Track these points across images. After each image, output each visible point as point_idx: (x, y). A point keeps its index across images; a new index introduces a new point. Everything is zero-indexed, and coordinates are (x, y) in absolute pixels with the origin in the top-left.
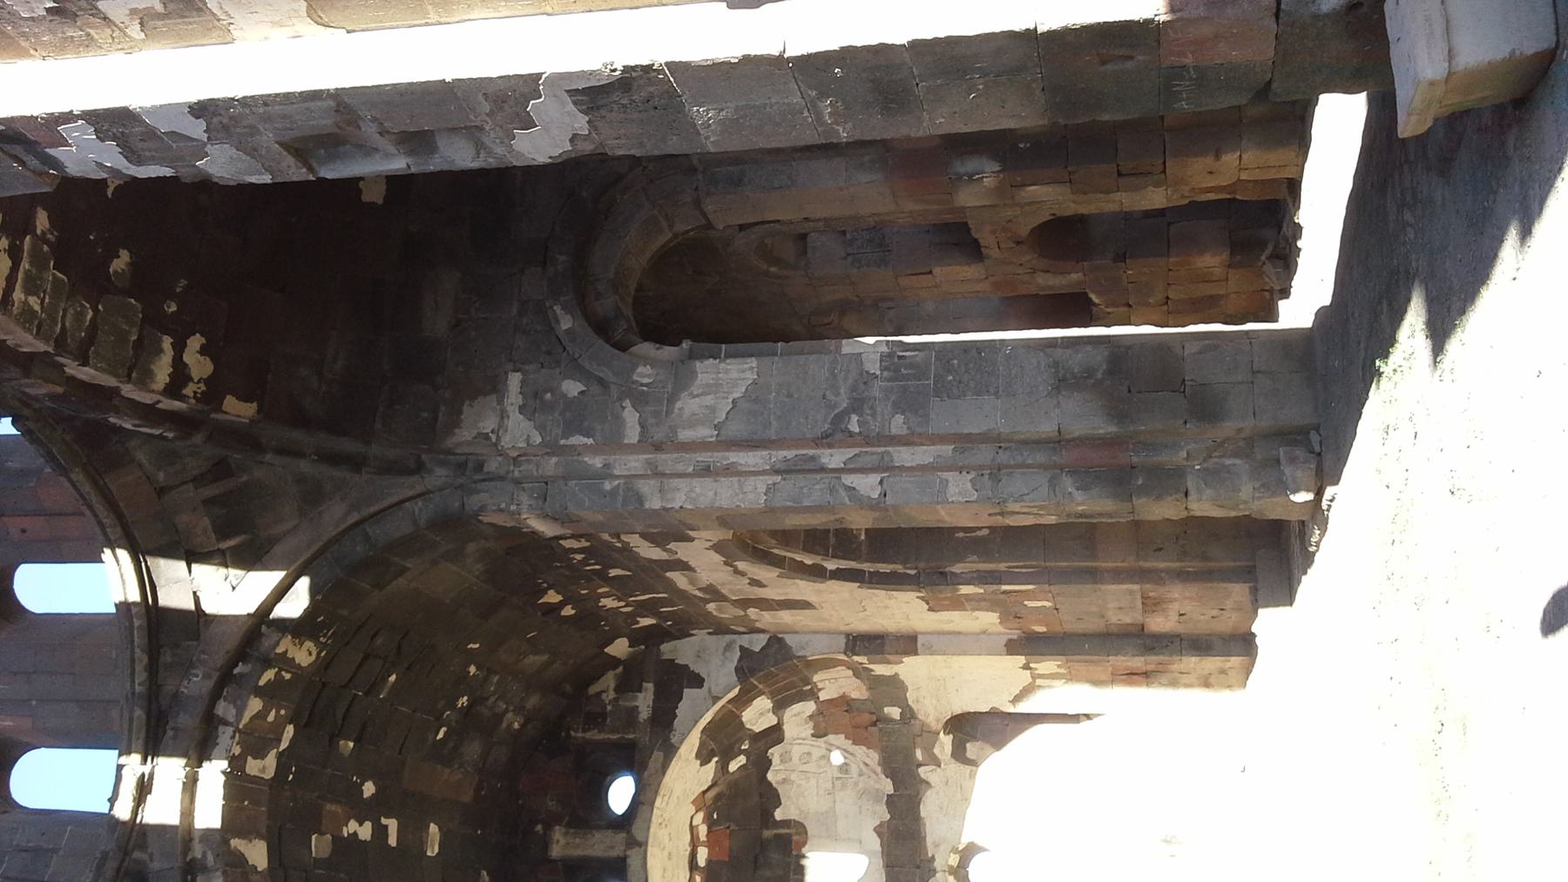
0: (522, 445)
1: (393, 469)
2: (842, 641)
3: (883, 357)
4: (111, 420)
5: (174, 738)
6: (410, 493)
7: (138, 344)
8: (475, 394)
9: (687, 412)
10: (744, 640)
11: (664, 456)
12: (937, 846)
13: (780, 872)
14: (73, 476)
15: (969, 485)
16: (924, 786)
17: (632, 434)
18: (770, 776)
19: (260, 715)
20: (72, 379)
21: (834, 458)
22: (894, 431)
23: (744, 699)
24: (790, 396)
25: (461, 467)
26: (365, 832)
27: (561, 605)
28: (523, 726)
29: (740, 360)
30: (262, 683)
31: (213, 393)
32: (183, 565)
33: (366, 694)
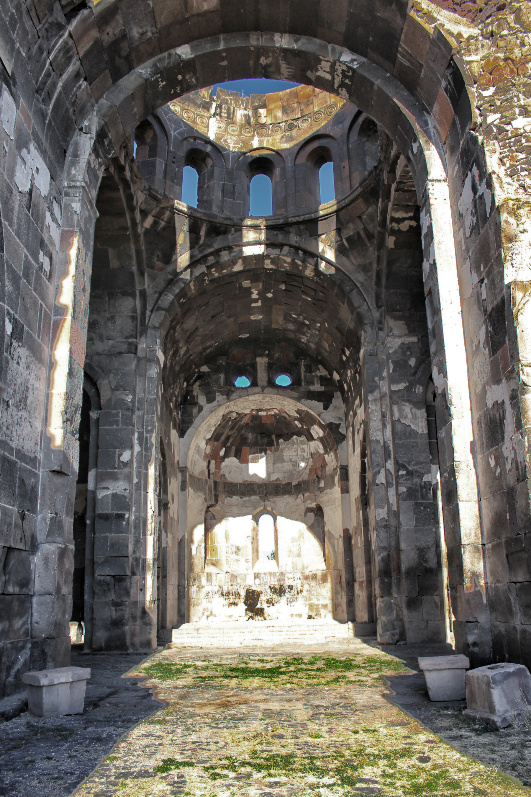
0: (388, 346)
1: (378, 297)
2: (345, 464)
3: (430, 483)
4: (380, 200)
5: (274, 235)
6: (369, 304)
7: (408, 206)
8: (408, 324)
9: (404, 408)
11: (388, 400)
12: (274, 502)
13: (260, 442)
14: (359, 188)
15: (382, 517)
16: (295, 496)
17: (395, 388)
18: (295, 437)
19: (285, 262)
20: (391, 186)
21: (390, 465)
22: (400, 488)
23: (321, 426)
24: (413, 447)
25: (380, 322)
26: (255, 296)
27: (346, 356)
28: (303, 343)
29: (426, 426)
30: (296, 261)
31: (393, 232)
32: (335, 228)
33: (302, 291)
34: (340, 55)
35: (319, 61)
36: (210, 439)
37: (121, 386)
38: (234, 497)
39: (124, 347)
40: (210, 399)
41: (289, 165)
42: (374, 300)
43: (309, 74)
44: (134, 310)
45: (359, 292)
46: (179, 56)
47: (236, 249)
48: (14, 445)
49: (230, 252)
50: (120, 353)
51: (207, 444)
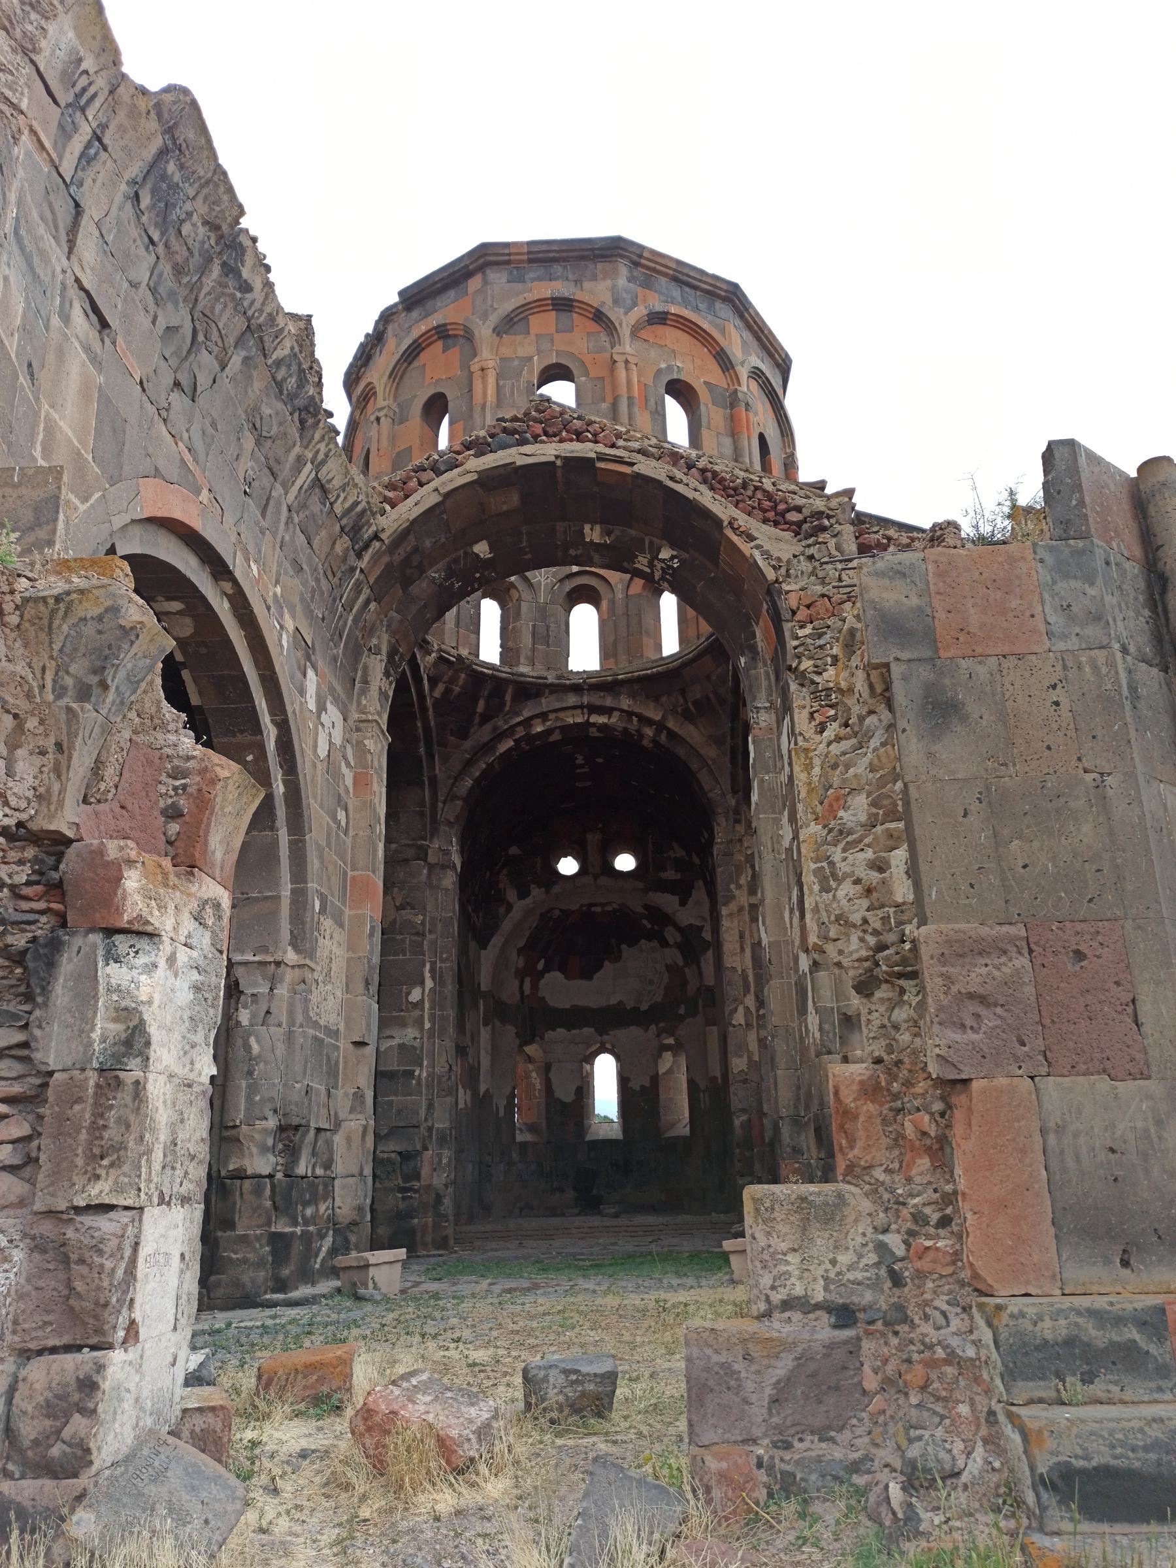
0: (746, 844)
10: (708, 927)
18: (643, 941)
21: (750, 1001)
26: (580, 760)
34: (659, 552)
35: (637, 556)
36: (523, 948)
37: (408, 903)
38: (559, 1030)
39: (411, 852)
40: (523, 894)
41: (620, 595)
42: (729, 782)
43: (625, 564)
44: (422, 804)
45: (710, 771)
46: (477, 555)
47: (552, 716)
48: (322, 1022)
49: (544, 721)
50: (406, 861)
51: (519, 955)
